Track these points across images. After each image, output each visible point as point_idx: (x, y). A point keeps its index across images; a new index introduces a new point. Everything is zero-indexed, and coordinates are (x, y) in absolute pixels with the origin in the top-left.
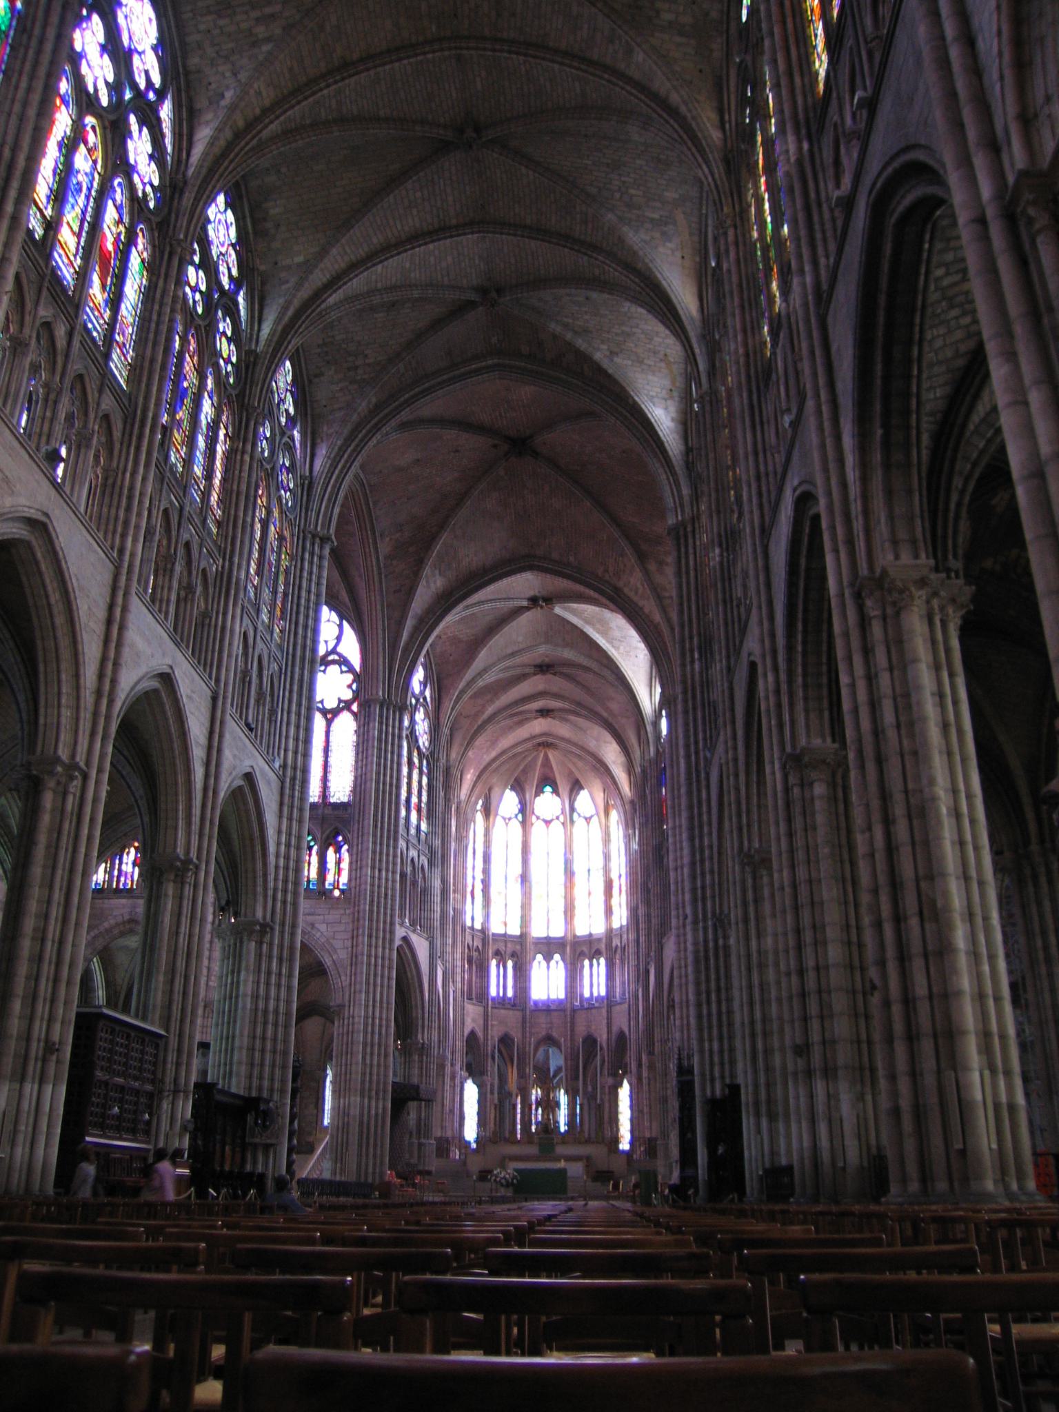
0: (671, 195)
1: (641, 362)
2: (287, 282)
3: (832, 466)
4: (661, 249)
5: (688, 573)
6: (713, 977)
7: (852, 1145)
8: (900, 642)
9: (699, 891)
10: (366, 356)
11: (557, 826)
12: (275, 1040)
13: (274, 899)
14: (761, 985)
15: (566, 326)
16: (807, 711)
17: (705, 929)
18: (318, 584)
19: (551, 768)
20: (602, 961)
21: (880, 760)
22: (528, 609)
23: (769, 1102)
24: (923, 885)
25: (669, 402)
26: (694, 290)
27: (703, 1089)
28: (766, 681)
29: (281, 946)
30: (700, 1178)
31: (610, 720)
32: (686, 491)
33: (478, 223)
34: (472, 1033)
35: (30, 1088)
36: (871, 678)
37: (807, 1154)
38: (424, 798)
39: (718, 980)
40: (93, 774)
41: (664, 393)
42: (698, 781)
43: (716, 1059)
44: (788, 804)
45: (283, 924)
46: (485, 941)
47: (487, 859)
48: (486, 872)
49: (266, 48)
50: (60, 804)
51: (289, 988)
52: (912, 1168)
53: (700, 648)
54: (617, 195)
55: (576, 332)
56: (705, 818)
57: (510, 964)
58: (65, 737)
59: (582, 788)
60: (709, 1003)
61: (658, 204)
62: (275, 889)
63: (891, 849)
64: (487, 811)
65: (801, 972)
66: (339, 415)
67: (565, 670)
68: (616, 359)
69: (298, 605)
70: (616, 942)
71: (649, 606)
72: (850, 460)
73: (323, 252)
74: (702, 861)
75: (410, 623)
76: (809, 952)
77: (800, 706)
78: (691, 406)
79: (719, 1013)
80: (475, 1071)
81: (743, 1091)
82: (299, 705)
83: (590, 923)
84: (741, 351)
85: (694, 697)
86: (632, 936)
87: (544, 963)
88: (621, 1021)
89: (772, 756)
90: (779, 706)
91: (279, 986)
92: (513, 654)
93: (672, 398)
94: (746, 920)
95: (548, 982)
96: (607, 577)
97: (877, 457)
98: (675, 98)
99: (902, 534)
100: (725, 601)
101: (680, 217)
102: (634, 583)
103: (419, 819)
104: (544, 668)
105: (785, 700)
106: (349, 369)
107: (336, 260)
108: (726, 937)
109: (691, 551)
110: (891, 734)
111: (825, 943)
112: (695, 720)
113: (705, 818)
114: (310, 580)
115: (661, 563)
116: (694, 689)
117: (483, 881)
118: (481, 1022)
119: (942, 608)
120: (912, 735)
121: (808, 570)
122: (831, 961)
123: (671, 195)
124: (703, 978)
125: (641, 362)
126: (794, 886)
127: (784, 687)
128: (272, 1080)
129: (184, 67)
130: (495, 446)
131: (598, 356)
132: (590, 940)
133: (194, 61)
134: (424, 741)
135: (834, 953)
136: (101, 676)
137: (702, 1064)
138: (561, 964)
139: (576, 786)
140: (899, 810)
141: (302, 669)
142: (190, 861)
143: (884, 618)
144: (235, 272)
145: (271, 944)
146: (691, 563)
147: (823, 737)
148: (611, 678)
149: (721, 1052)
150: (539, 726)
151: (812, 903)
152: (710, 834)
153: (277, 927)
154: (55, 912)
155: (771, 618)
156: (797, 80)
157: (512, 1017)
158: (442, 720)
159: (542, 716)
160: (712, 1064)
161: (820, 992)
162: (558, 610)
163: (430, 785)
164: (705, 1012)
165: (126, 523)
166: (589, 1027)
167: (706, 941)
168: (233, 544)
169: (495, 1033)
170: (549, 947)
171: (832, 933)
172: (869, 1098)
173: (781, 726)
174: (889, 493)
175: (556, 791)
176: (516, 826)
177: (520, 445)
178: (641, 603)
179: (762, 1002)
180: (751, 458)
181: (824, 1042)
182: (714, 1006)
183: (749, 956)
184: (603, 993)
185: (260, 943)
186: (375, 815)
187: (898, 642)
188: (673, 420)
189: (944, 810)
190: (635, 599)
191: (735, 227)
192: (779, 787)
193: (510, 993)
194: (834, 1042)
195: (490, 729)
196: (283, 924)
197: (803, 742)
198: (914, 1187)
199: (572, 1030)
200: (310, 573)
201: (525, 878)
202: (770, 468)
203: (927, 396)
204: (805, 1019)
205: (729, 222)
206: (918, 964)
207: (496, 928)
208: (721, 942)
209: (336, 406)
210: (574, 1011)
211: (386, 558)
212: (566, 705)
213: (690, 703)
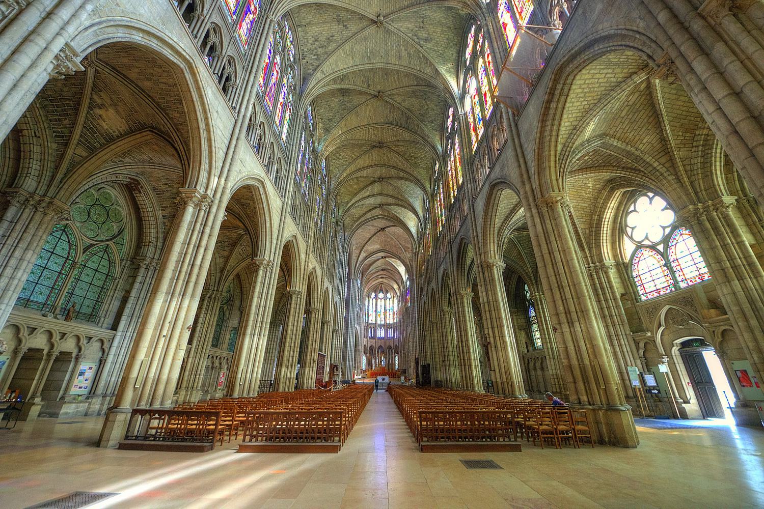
0: (418, 192)
11: (383, 300)
33: (380, 194)
35: (311, 369)
58: (316, 304)
64: (369, 296)
65: (444, 348)
83: (390, 321)
95: (381, 333)
101: (419, 196)
104: (383, 270)
107: (353, 201)
123: (418, 192)
132: (390, 324)
133: (331, 168)
134: (359, 285)
154: (315, 336)
169: (370, 345)
170: (381, 326)
175: (383, 293)
176: (374, 300)
177: (383, 229)
207: (370, 322)
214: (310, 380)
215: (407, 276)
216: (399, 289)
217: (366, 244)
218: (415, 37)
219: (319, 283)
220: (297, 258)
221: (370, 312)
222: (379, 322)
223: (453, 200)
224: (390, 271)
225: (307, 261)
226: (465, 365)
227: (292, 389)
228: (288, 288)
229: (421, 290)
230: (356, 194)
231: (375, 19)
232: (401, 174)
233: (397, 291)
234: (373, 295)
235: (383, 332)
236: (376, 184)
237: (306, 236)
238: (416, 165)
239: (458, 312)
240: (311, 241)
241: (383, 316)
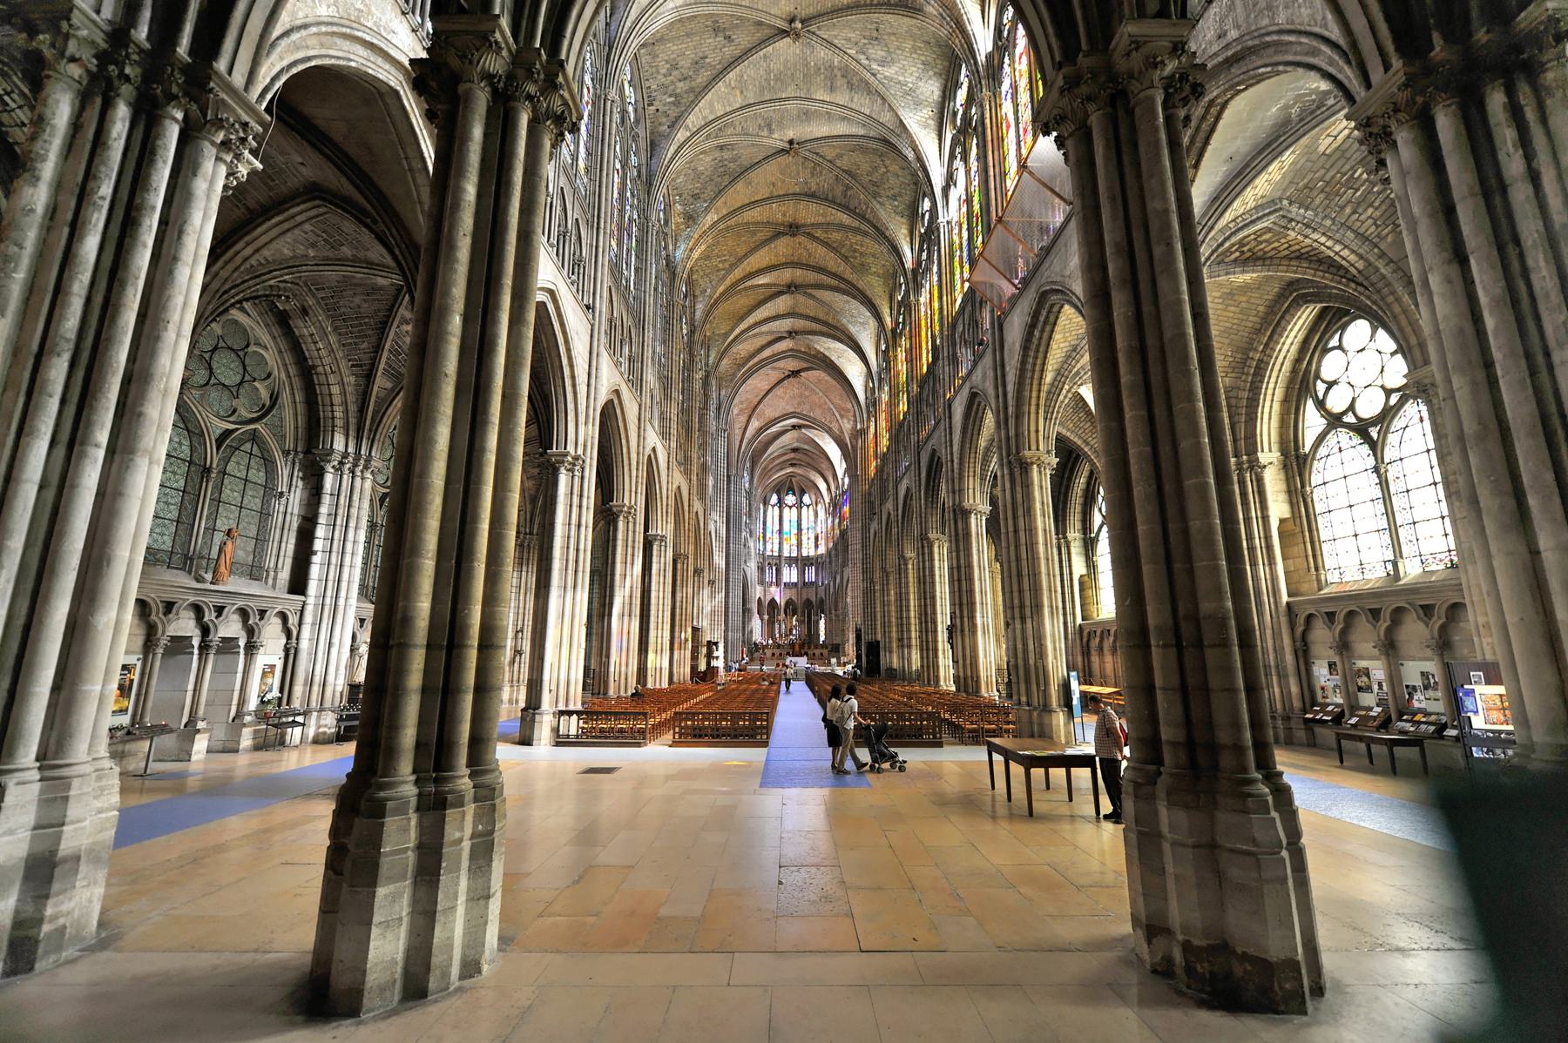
33: (791, 314)
64: (766, 502)
73: (732, 330)
83: (808, 550)
88: (822, 594)
104: (795, 450)
107: (737, 331)
150: (790, 470)
169: (768, 598)
170: (791, 561)
177: (795, 373)
187: (931, 553)
216: (829, 489)
217: (760, 402)
218: (862, 57)
221: (768, 535)
222: (786, 554)
227: (665, 685)
230: (742, 318)
231: (784, 25)
232: (834, 282)
234: (774, 499)
235: (794, 572)
236: (783, 297)
238: (863, 268)
240: (673, 445)
241: (794, 541)
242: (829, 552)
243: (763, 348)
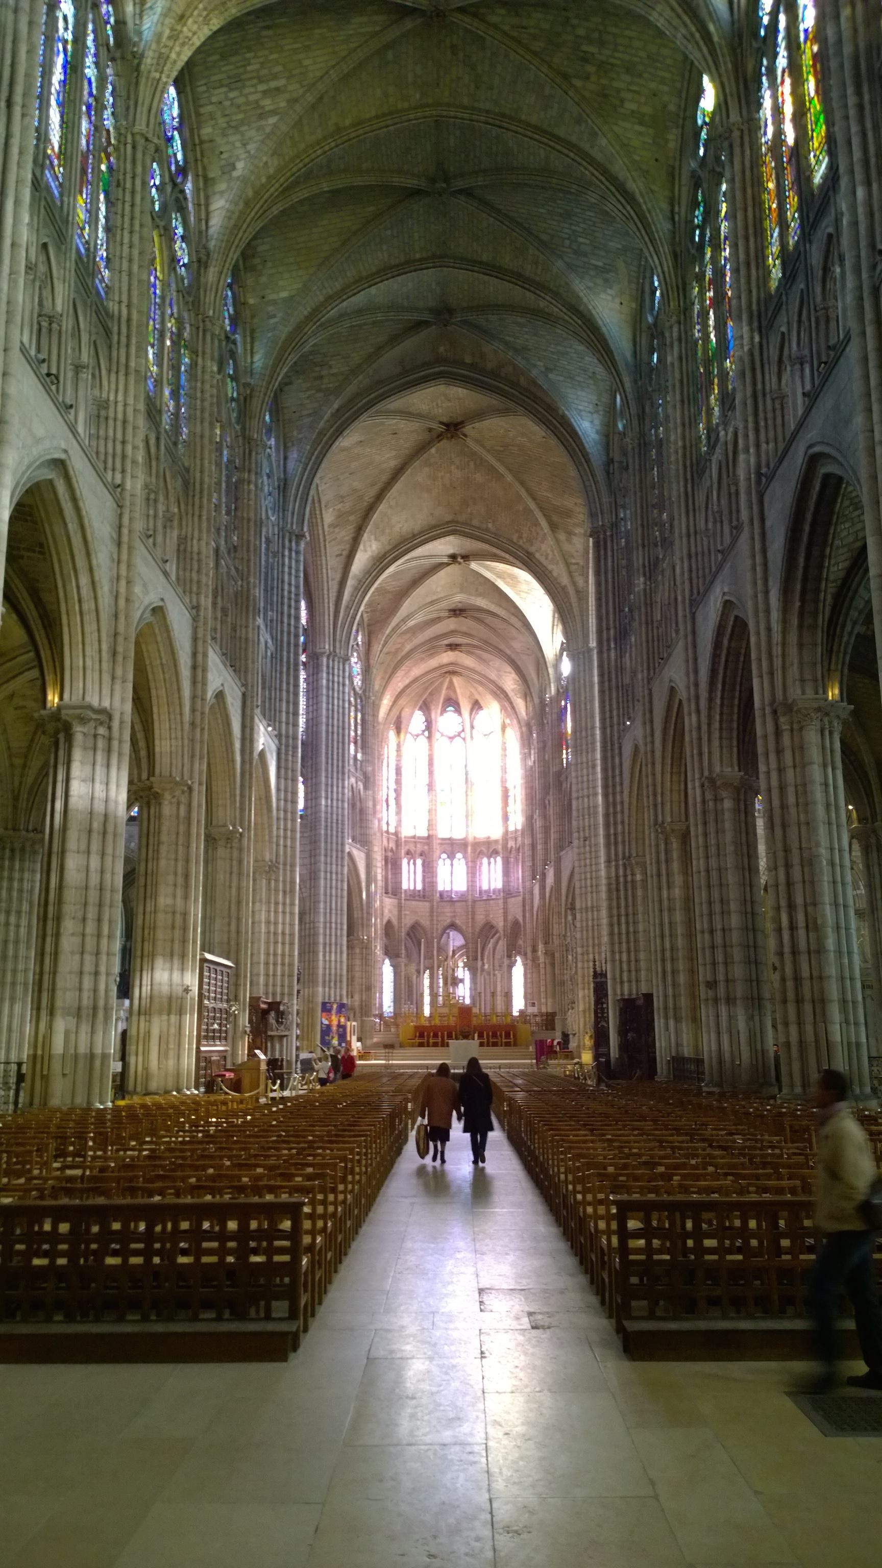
0: (614, 245)
1: (572, 379)
2: (274, 316)
3: (761, 615)
4: (603, 296)
5: (606, 573)
6: (623, 904)
7: (745, 1048)
8: (802, 748)
9: (612, 837)
10: (331, 367)
12: (283, 955)
13: (278, 845)
14: (670, 923)
15: (506, 343)
16: (721, 747)
17: (617, 867)
18: (297, 577)
19: (455, 691)
20: (499, 859)
21: (784, 826)
22: (448, 564)
23: (675, 1008)
24: (810, 909)
25: (595, 416)
26: (630, 336)
27: (614, 990)
28: (690, 719)
29: (284, 881)
30: (612, 1055)
31: (513, 656)
32: (606, 500)
33: (439, 258)
34: (389, 922)
36: (781, 770)
37: (714, 1054)
38: (359, 732)
39: (627, 906)
40: (196, 787)
41: (591, 408)
42: (612, 750)
43: (625, 967)
44: (704, 812)
45: (285, 864)
46: (398, 842)
47: (398, 771)
48: (398, 782)
49: (272, 120)
50: (175, 812)
51: (292, 914)
52: (797, 1080)
53: (615, 639)
54: (567, 243)
55: (516, 350)
56: (618, 779)
57: (419, 862)
59: (480, 708)
60: (619, 924)
61: (602, 253)
62: (278, 836)
63: (789, 884)
65: (712, 932)
66: (307, 420)
67: (476, 614)
68: (550, 376)
69: (283, 597)
70: (511, 844)
71: (558, 571)
72: (775, 615)
74: (615, 813)
75: (350, 583)
76: (717, 918)
77: (716, 743)
78: (615, 425)
79: (628, 933)
80: (391, 952)
81: (655, 999)
82: (288, 684)
84: (680, 443)
85: (610, 680)
86: (527, 841)
87: (448, 861)
88: (516, 911)
89: (694, 775)
90: (700, 739)
91: (284, 912)
92: (432, 603)
93: (597, 412)
94: (659, 875)
95: (452, 877)
96: (521, 543)
97: (795, 622)
98: (632, 186)
99: (808, 676)
100: (647, 623)
101: (621, 265)
102: (545, 549)
103: (356, 751)
104: (457, 612)
105: (705, 737)
106: (316, 378)
108: (633, 875)
109: (609, 553)
110: (793, 810)
111: (729, 913)
112: (610, 700)
113: (618, 779)
114: (290, 574)
115: (570, 533)
116: (609, 673)
117: (396, 790)
118: (396, 912)
119: (830, 722)
120: (806, 812)
121: (729, 648)
122: (733, 926)
124: (615, 904)
125: (572, 379)
126: (708, 871)
127: (704, 728)
128: (282, 986)
129: (199, 136)
130: (430, 430)
131: (534, 373)
132: (488, 843)
133: (207, 131)
134: (358, 681)
135: (735, 920)
136: (193, 710)
137: (613, 970)
138: (463, 861)
139: (476, 706)
140: (796, 860)
141: (289, 652)
142: (235, 831)
143: (792, 730)
144: (231, 311)
145: (277, 881)
146: (610, 564)
147: (732, 766)
148: (519, 624)
149: (629, 962)
150: (447, 657)
151: (721, 885)
152: (622, 792)
153: (281, 867)
155: (696, 672)
156: (754, 272)
157: (423, 907)
158: (371, 662)
159: (452, 650)
160: (621, 971)
161: (725, 946)
162: (474, 565)
163: (363, 720)
164: (616, 931)
165: (199, 582)
166: (487, 915)
167: (617, 877)
168: (248, 567)
169: (408, 921)
170: (453, 847)
171: (733, 906)
172: (757, 1018)
173: (700, 754)
174: (801, 645)
175: (458, 711)
176: (423, 740)
177: (452, 428)
178: (550, 567)
179: (671, 936)
180: (684, 539)
181: (727, 981)
182: (624, 927)
183: (661, 901)
184: (499, 885)
185: (269, 881)
186: (327, 753)
187: (800, 748)
188: (597, 432)
189: (825, 863)
190: (545, 563)
191: (679, 323)
192: (699, 799)
193: (419, 887)
194: (734, 981)
195: (408, 663)
196: (285, 864)
197: (718, 769)
198: (798, 1090)
199: (473, 918)
200: (290, 568)
201: (431, 787)
202: (699, 549)
203: (833, 569)
204: (714, 964)
205: (674, 318)
206: (804, 958)
207: (407, 832)
208: (629, 878)
209: (305, 412)
210: (474, 901)
211: (330, 526)
212: (475, 642)
213: (607, 684)
214: (171, 1063)
215: (559, 638)
217: (380, 497)
219: (185, 673)
220: (81, 562)
223: (776, 273)
224: (489, 619)
225: (124, 577)
226: (799, 1001)
228: (53, 698)
229: (619, 693)
233: (520, 704)
237: (101, 463)
239: (782, 788)
240: (136, 484)
242: (530, 819)
243: (379, 350)
